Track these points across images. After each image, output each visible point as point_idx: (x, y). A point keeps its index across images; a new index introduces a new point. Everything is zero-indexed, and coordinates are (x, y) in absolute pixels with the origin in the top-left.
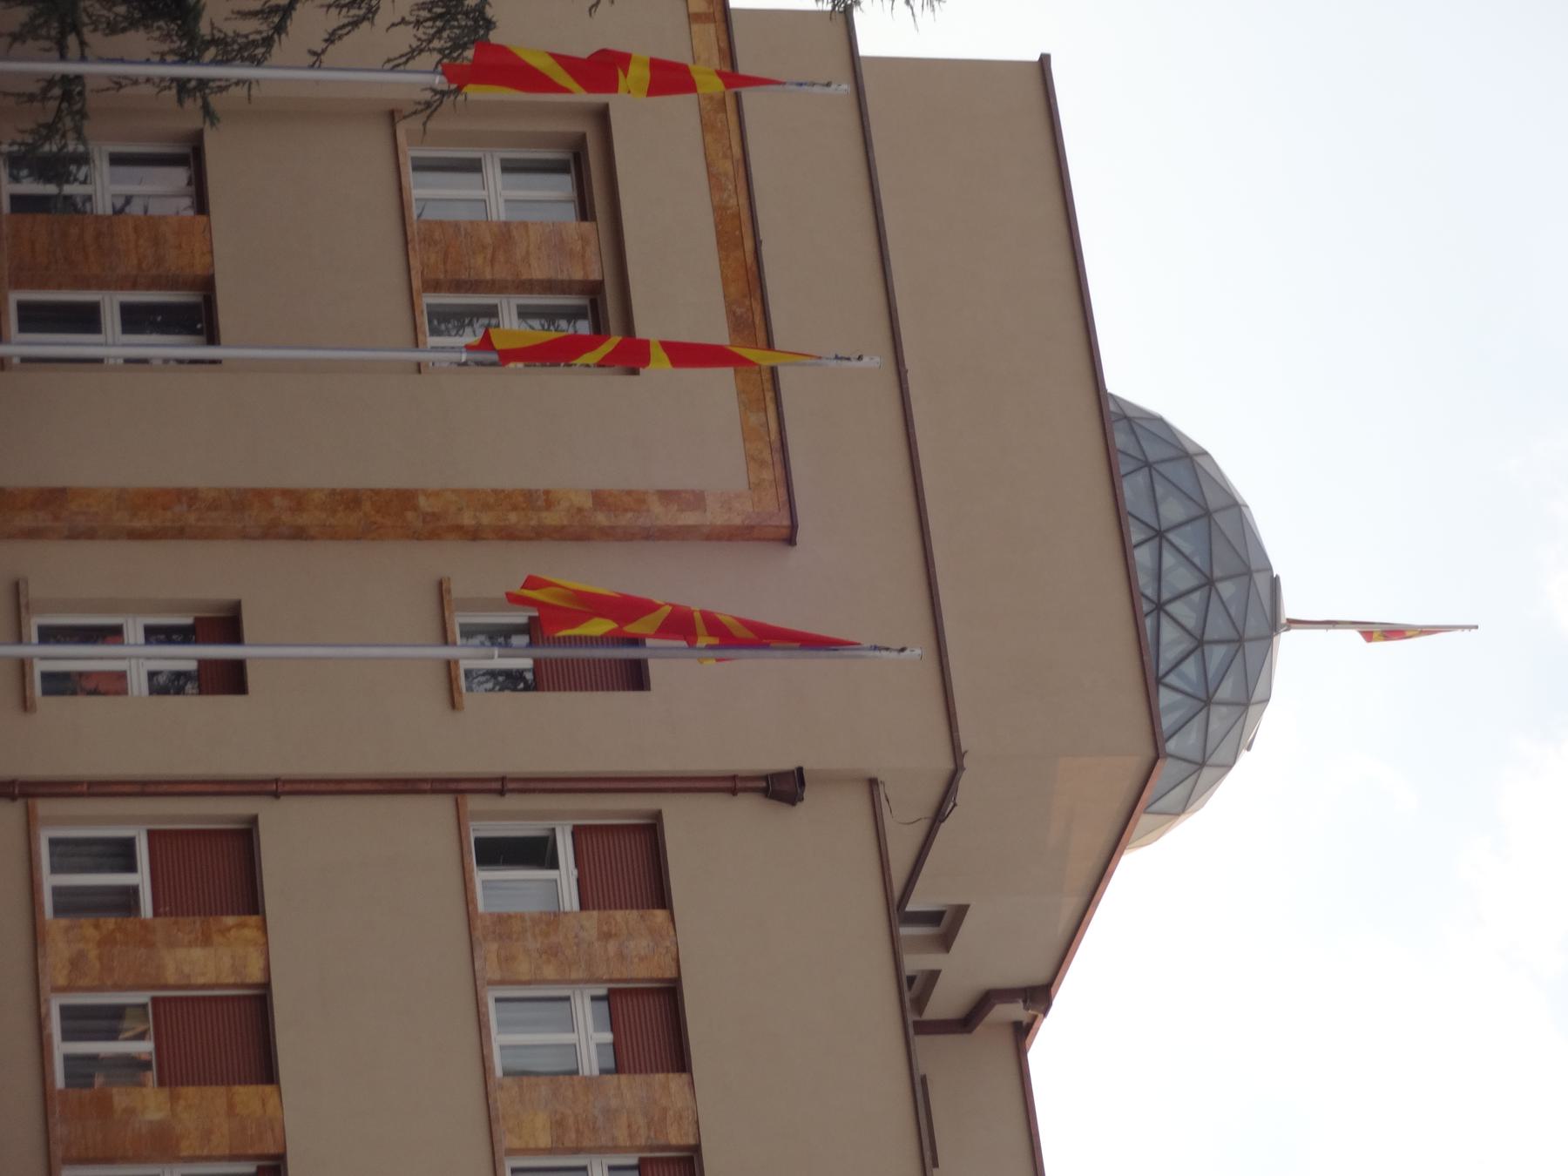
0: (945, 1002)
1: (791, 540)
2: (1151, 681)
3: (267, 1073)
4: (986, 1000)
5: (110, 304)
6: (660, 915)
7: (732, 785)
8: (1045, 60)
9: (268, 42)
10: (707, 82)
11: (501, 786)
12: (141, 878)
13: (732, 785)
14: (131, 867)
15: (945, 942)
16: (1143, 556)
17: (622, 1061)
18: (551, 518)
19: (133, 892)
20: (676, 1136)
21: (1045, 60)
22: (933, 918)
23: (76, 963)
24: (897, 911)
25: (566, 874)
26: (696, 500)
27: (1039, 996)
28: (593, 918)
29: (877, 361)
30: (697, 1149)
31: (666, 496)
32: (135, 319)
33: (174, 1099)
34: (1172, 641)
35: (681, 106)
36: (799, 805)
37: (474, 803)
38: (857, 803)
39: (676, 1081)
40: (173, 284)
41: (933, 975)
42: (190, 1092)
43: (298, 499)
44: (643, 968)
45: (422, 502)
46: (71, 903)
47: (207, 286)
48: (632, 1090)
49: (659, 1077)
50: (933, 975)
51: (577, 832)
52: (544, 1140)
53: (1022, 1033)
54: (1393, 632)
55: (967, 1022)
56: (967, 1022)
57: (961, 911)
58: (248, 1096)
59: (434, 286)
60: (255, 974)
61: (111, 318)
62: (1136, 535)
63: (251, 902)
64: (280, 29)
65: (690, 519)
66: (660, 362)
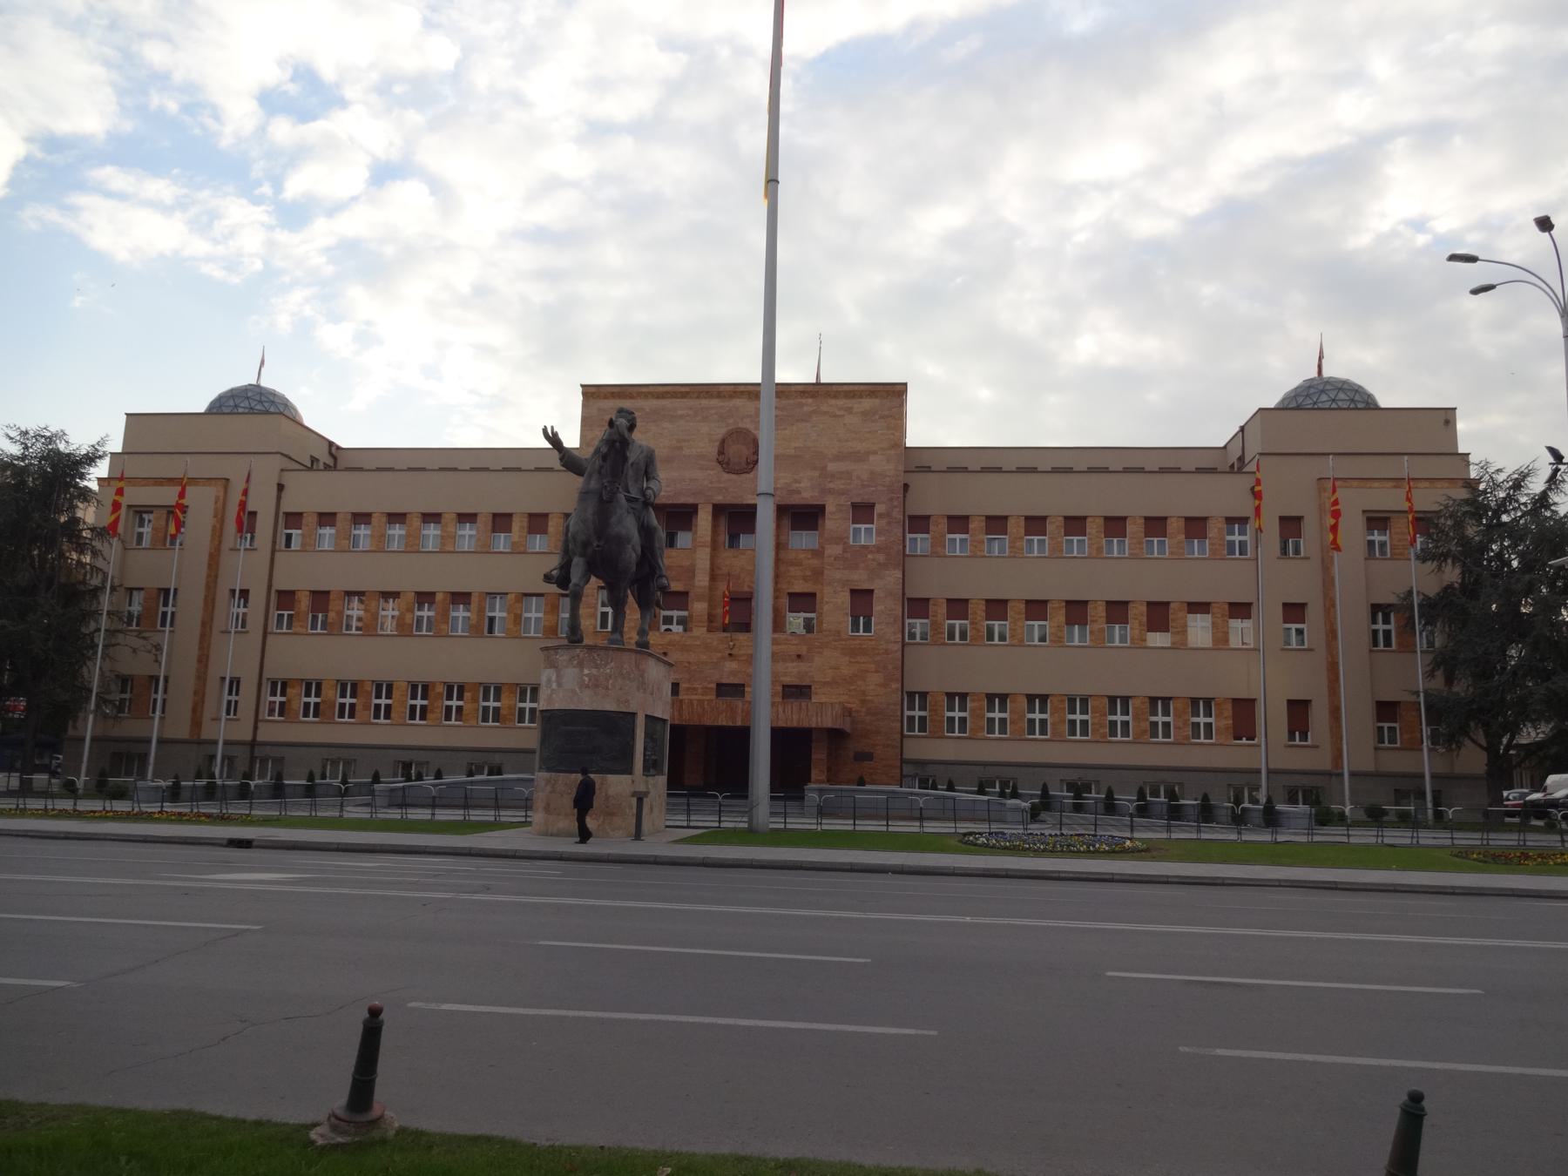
0: (330, 462)
1: (228, 480)
2: (267, 412)
3: (328, 593)
4: (331, 454)
5: (162, 609)
6: (305, 515)
7: (279, 498)
8: (127, 414)
9: (104, 573)
10: (121, 484)
11: (274, 542)
12: (286, 613)
13: (279, 498)
15: (318, 460)
16: (240, 410)
17: (332, 525)
18: (218, 526)
19: (289, 615)
20: (349, 517)
21: (127, 414)
22: (312, 462)
23: (301, 626)
24: (310, 469)
25: (294, 532)
26: (217, 498)
27: (331, 444)
28: (303, 527)
29: (188, 458)
30: (352, 513)
31: (216, 503)
32: (166, 604)
33: (332, 610)
34: (258, 407)
35: (127, 490)
36: (286, 486)
37: (277, 547)
38: (286, 473)
40: (159, 596)
41: (325, 464)
42: (330, 607)
43: (209, 576)
44: (315, 519)
45: (213, 551)
46: (289, 626)
47: (160, 589)
48: (338, 524)
49: (337, 519)
50: (325, 464)
51: (286, 529)
52: (348, 542)
53: (338, 448)
54: (262, 363)
55: (335, 458)
56: (335, 458)
57: (311, 456)
59: (165, 545)
60: (308, 593)
61: (165, 609)
62: (236, 411)
64: (101, 570)
65: (221, 498)
66: (185, 502)
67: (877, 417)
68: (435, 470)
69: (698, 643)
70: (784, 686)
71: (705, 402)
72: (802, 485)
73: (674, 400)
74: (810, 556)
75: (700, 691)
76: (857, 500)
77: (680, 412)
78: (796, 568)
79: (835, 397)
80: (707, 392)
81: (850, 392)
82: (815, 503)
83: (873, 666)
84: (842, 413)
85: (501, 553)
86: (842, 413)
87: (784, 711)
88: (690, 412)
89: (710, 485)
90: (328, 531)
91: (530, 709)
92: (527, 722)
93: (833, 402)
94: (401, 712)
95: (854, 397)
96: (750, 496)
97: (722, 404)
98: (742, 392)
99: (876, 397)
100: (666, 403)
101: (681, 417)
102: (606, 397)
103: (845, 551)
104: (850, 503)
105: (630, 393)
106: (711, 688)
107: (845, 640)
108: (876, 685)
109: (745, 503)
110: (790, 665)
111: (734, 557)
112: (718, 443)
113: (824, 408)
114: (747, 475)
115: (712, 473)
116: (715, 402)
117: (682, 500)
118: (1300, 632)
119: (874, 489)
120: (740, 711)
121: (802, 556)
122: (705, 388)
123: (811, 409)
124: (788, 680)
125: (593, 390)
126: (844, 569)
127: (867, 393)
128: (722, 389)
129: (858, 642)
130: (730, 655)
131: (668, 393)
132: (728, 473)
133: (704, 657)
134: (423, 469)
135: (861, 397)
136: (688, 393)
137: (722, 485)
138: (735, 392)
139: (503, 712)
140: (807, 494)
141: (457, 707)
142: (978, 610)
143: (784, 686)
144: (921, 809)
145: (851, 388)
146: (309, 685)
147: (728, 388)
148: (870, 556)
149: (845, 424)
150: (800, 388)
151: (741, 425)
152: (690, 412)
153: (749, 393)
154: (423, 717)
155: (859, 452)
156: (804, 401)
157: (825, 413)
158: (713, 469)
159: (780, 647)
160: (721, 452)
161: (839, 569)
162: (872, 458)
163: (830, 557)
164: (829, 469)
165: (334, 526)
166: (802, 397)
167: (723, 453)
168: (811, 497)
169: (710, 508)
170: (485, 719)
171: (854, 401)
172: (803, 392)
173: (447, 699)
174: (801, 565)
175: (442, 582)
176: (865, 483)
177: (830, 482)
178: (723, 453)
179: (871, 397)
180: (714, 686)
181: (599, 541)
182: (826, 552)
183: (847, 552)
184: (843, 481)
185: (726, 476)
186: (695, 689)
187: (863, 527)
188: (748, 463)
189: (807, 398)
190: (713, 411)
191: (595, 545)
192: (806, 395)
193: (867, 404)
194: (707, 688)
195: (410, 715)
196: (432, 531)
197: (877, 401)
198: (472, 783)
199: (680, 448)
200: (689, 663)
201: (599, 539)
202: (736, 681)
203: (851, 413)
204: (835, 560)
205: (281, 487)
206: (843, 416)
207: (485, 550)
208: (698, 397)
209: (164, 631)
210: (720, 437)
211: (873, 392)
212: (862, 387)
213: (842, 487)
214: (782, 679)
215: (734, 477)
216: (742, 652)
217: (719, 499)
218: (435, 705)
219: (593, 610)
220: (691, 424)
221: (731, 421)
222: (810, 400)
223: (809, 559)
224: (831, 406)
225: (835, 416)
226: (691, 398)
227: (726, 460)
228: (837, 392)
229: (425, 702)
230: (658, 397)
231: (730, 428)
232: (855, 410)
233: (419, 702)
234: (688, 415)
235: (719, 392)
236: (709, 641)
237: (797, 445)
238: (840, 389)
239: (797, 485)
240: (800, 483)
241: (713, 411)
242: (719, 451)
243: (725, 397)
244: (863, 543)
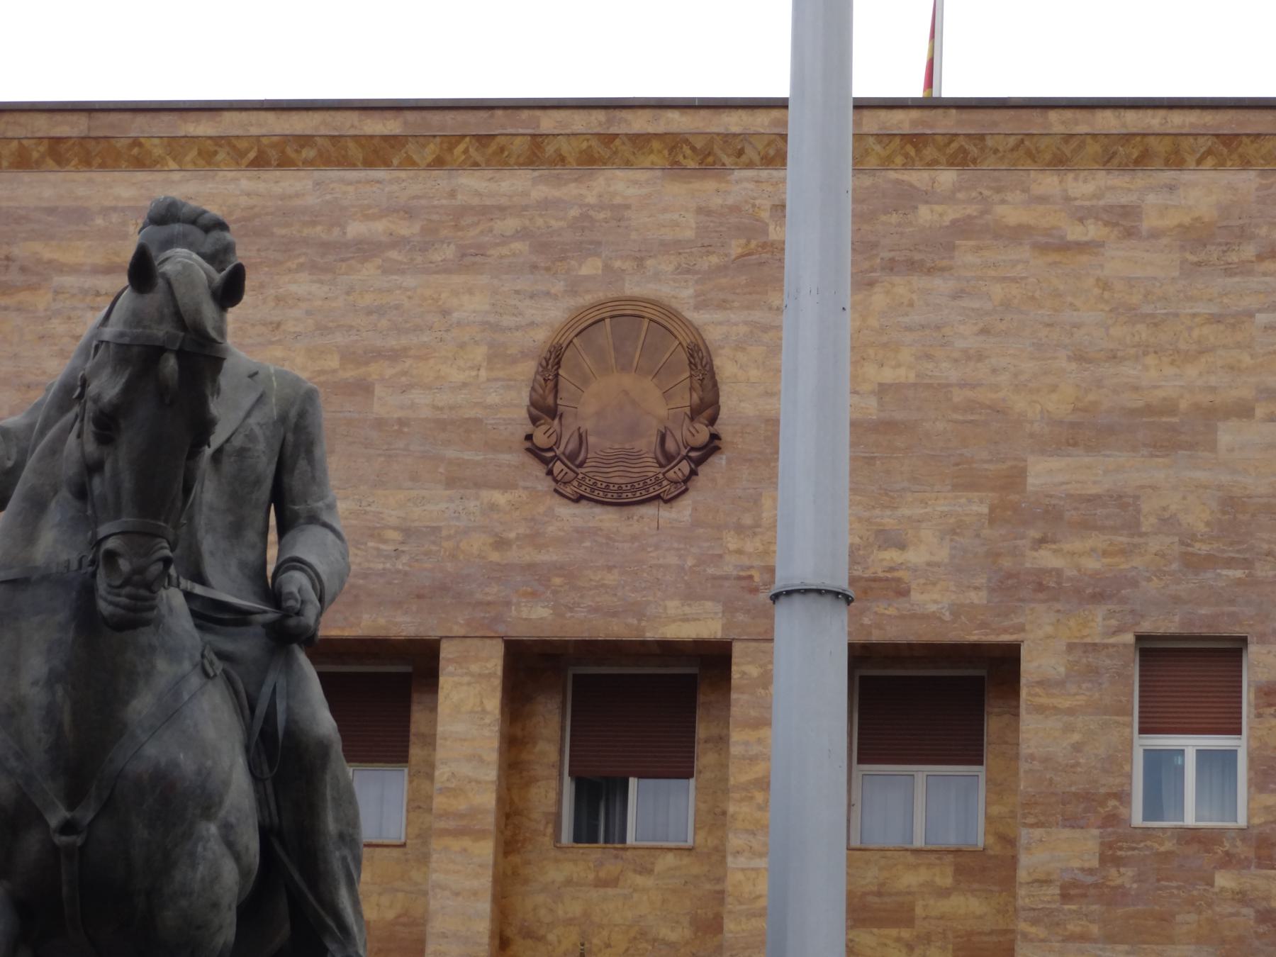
67: (1249, 251)
72: (915, 556)
73: (334, 174)
74: (947, 881)
77: (356, 229)
78: (894, 932)
79: (1059, 162)
80: (483, 140)
81: (1127, 137)
82: (975, 637)
84: (1092, 231)
86: (1092, 231)
88: (406, 229)
89: (495, 557)
93: (1048, 183)
95: (1142, 161)
96: (673, 606)
97: (541, 192)
98: (641, 141)
99: (1246, 164)
101: (365, 249)
103: (1109, 857)
104: (1129, 638)
105: (136, 142)
109: (650, 635)
111: (600, 883)
112: (528, 369)
113: (1011, 212)
114: (666, 514)
115: (500, 498)
119: (1239, 573)
121: (909, 880)
122: (477, 126)
123: (952, 213)
126: (1111, 939)
127: (1204, 144)
128: (548, 123)
131: (304, 140)
132: (578, 499)
135: (1175, 161)
137: (549, 556)
145: (1132, 121)
147: (580, 122)
148: (1224, 880)
149: (1105, 285)
151: (633, 287)
152: (406, 229)
153: (674, 143)
155: (1169, 408)
156: (918, 178)
157: (1017, 234)
158: (506, 486)
161: (1083, 937)
162: (1228, 435)
163: (1046, 882)
164: (1030, 480)
166: (908, 165)
167: (553, 413)
168: (957, 611)
169: (493, 660)
171: (1141, 179)
172: (916, 140)
174: (909, 922)
176: (1202, 548)
177: (1042, 541)
178: (553, 413)
179: (1220, 165)
181: (71, 806)
182: (1024, 860)
183: (1118, 862)
184: (1097, 541)
185: (570, 515)
187: (1190, 744)
188: (668, 458)
189: (932, 164)
190: (510, 224)
191: (54, 821)
192: (930, 152)
197: (1246, 181)
199: (363, 388)
201: (74, 798)
203: (1130, 233)
204: (1065, 897)
206: (1082, 247)
208: (439, 163)
210: (541, 337)
211: (1230, 140)
212: (1178, 120)
213: (1092, 564)
215: (606, 518)
220: (409, 281)
221: (591, 267)
222: (947, 177)
223: (944, 893)
224: (1043, 199)
225: (1066, 247)
226: (409, 163)
227: (568, 444)
228: (1070, 137)
230: (260, 162)
231: (588, 299)
232: (1150, 222)
234: (398, 242)
235: (537, 140)
237: (888, 375)
238: (1083, 124)
239: (891, 556)
240: (902, 547)
241: (510, 224)
242: (533, 404)
243: (561, 160)
244: (1190, 820)
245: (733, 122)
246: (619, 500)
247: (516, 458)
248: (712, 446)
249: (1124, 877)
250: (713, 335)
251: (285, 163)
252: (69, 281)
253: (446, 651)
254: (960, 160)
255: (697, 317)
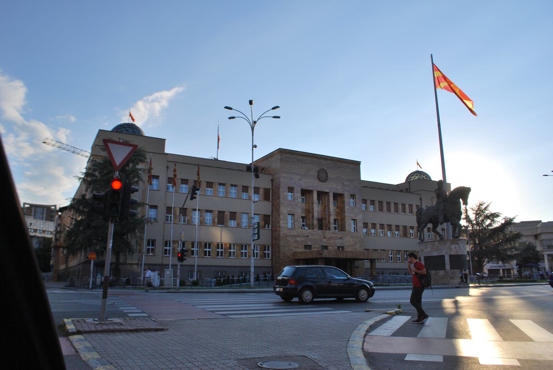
14: (168, 216)
20: (193, 181)
39: (189, 181)
58: (188, 210)
60: (179, 209)
63: (235, 213)
66: (175, 173)
68: (226, 169)
69: (316, 233)
70: (338, 247)
71: (314, 159)
75: (317, 248)
76: (351, 193)
77: (307, 161)
79: (345, 163)
83: (358, 241)
85: (184, 193)
87: (375, 255)
90: (184, 186)
91: (208, 251)
92: (232, 256)
94: (213, 254)
100: (303, 158)
102: (287, 153)
106: (320, 247)
107: (351, 234)
108: (359, 247)
110: (339, 240)
115: (316, 181)
116: (316, 160)
117: (309, 189)
118: (429, 234)
120: (366, 255)
124: (339, 245)
125: (283, 150)
128: (318, 156)
129: (354, 234)
130: (325, 237)
131: (303, 155)
133: (318, 238)
134: (232, 169)
136: (309, 155)
138: (321, 157)
139: (203, 254)
140: (340, 191)
141: (152, 249)
142: (378, 226)
143: (338, 247)
144: (407, 280)
146: (242, 246)
148: (355, 210)
150: (337, 159)
151: (323, 168)
153: (325, 158)
154: (209, 255)
156: (338, 163)
159: (336, 235)
160: (318, 176)
165: (187, 184)
170: (218, 255)
173: (165, 246)
175: (227, 208)
180: (320, 246)
186: (316, 247)
193: (353, 166)
194: (319, 247)
195: (269, 254)
196: (221, 189)
198: (397, 276)
200: (314, 239)
202: (326, 245)
205: (168, 167)
207: (239, 198)
209: (171, 223)
214: (337, 244)
215: (322, 183)
216: (327, 236)
217: (319, 189)
218: (227, 251)
219: (287, 221)
222: (339, 163)
229: (218, 250)
233: (207, 250)
235: (317, 157)
236: (319, 232)
239: (337, 187)
243: (318, 158)
245: (328, 157)
246: (322, 181)
247: (317, 178)
248: (327, 179)
249: (350, 209)
250: (327, 171)
251: (302, 156)
252: (290, 162)
253: (314, 191)
254: (340, 162)
255: (327, 170)
